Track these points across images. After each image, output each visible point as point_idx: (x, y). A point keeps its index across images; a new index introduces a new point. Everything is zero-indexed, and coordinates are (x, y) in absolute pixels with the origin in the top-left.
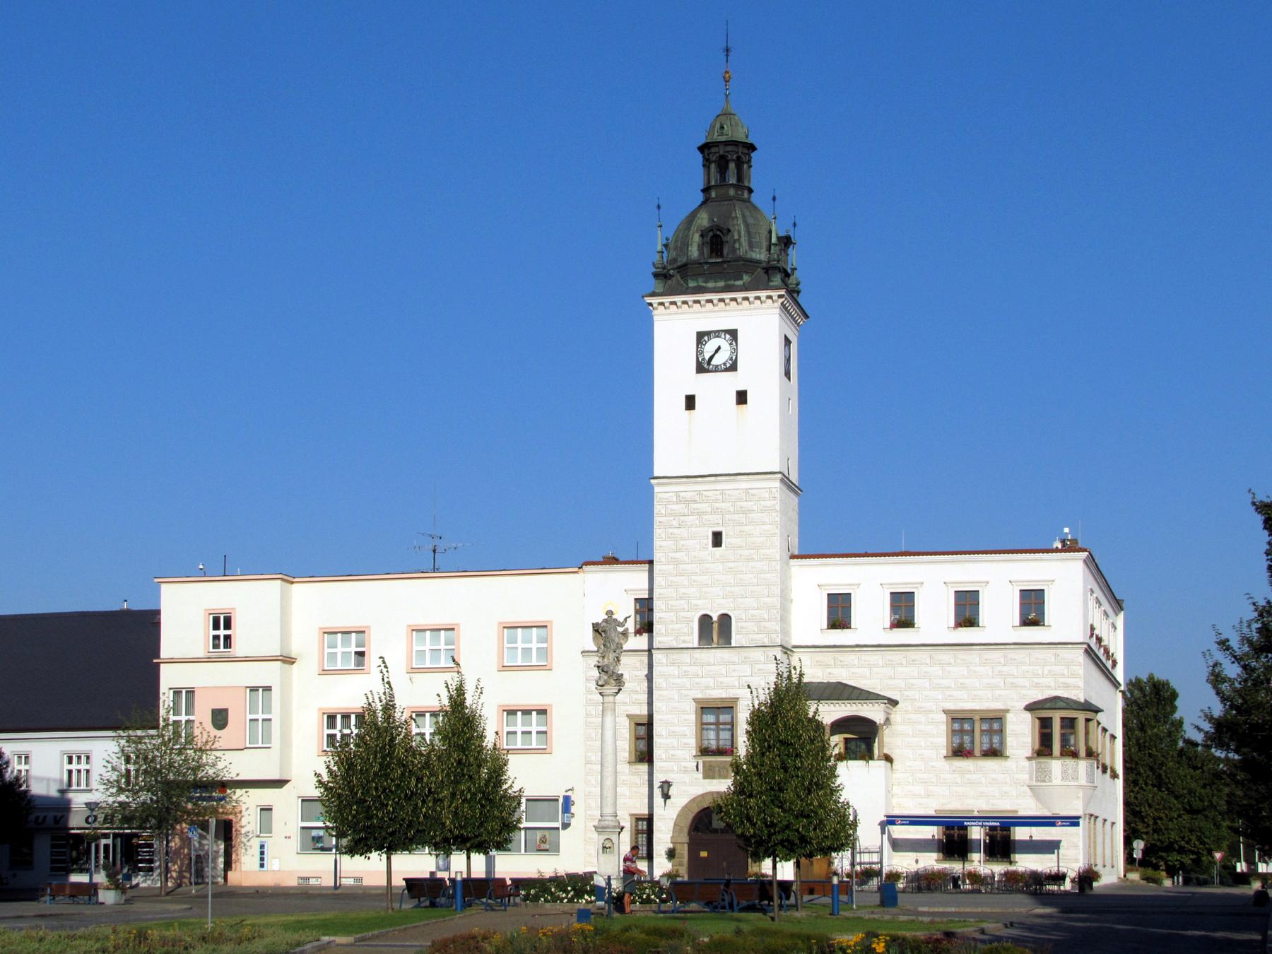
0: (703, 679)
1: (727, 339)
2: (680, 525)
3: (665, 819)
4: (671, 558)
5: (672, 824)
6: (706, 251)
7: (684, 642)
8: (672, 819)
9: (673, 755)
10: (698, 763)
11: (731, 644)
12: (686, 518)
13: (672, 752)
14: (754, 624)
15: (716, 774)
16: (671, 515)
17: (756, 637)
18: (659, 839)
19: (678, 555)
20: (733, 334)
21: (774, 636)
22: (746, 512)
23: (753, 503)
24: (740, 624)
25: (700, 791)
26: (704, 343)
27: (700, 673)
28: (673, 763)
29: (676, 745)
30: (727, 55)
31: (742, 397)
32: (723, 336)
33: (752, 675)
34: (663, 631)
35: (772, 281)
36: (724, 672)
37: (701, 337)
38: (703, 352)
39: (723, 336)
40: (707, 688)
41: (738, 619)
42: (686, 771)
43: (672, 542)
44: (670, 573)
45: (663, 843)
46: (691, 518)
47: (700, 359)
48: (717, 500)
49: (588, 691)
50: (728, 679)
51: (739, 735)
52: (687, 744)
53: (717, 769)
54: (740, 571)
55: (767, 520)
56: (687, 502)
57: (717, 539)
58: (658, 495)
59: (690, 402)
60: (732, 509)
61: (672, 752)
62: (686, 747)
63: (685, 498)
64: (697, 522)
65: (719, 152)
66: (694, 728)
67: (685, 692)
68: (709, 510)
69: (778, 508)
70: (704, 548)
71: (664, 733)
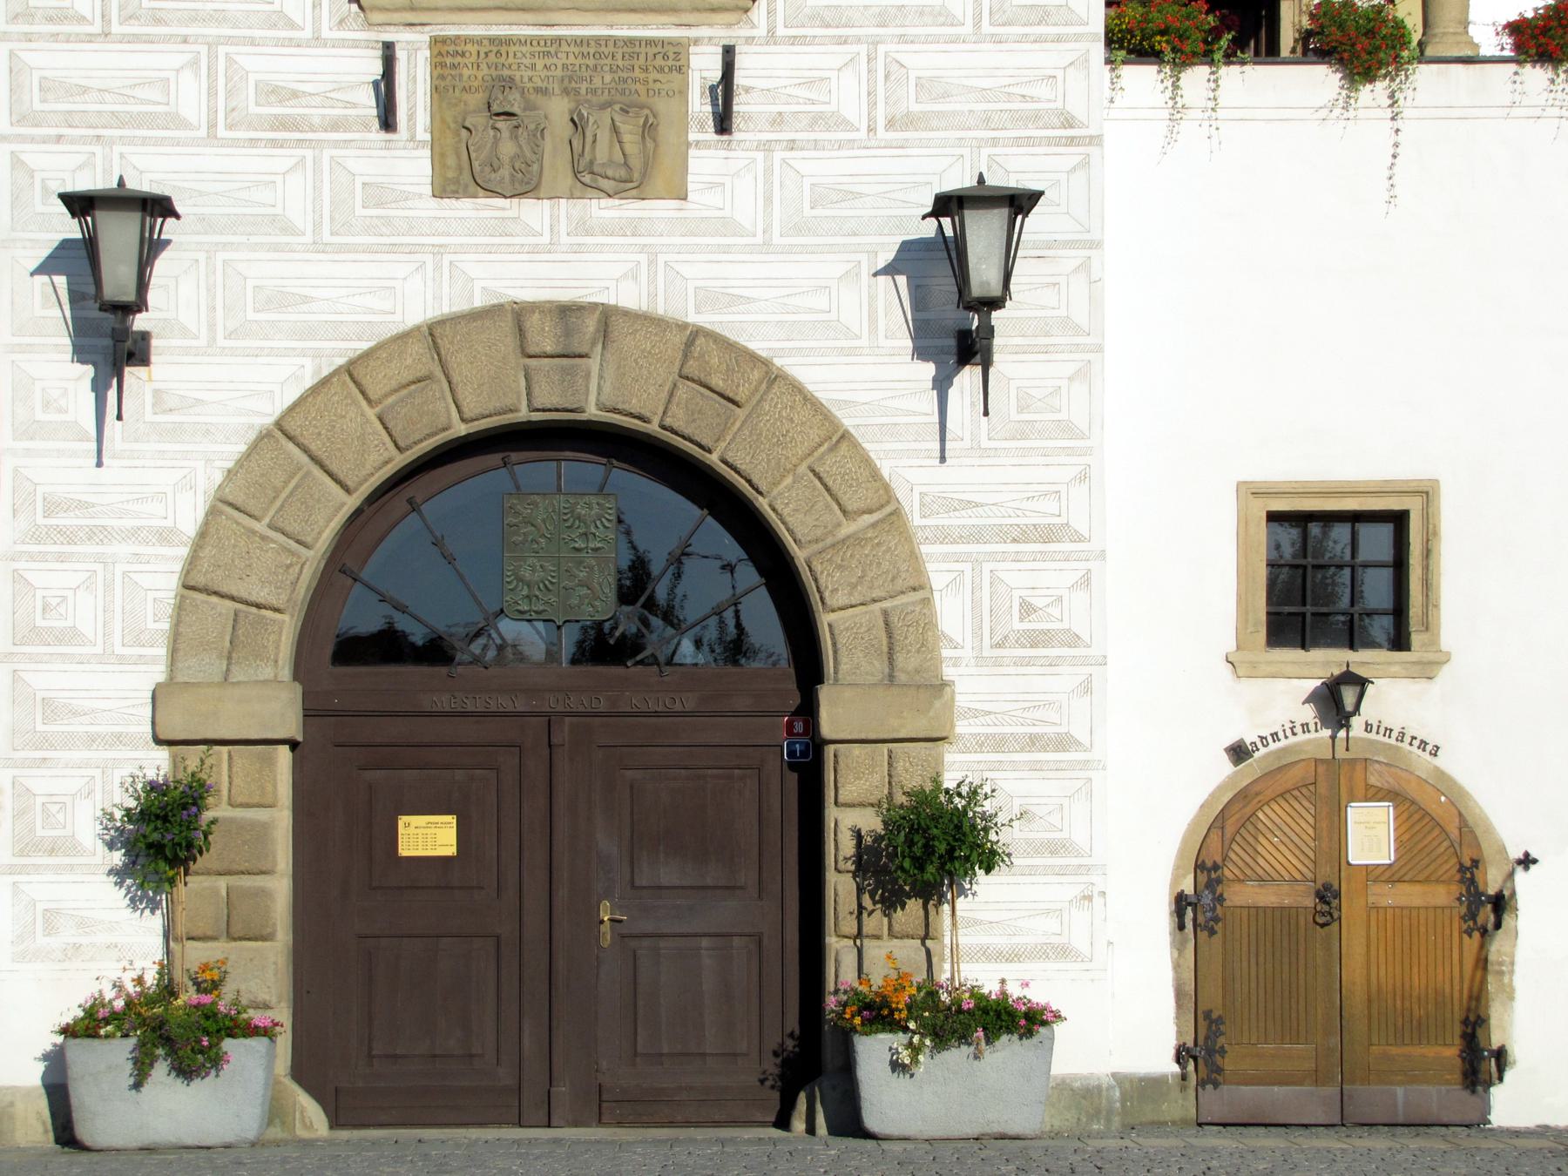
3: (99, 534)
5: (163, 581)
8: (165, 536)
10: (389, 54)
28: (168, 59)
45: (92, 740)
53: (558, 109)
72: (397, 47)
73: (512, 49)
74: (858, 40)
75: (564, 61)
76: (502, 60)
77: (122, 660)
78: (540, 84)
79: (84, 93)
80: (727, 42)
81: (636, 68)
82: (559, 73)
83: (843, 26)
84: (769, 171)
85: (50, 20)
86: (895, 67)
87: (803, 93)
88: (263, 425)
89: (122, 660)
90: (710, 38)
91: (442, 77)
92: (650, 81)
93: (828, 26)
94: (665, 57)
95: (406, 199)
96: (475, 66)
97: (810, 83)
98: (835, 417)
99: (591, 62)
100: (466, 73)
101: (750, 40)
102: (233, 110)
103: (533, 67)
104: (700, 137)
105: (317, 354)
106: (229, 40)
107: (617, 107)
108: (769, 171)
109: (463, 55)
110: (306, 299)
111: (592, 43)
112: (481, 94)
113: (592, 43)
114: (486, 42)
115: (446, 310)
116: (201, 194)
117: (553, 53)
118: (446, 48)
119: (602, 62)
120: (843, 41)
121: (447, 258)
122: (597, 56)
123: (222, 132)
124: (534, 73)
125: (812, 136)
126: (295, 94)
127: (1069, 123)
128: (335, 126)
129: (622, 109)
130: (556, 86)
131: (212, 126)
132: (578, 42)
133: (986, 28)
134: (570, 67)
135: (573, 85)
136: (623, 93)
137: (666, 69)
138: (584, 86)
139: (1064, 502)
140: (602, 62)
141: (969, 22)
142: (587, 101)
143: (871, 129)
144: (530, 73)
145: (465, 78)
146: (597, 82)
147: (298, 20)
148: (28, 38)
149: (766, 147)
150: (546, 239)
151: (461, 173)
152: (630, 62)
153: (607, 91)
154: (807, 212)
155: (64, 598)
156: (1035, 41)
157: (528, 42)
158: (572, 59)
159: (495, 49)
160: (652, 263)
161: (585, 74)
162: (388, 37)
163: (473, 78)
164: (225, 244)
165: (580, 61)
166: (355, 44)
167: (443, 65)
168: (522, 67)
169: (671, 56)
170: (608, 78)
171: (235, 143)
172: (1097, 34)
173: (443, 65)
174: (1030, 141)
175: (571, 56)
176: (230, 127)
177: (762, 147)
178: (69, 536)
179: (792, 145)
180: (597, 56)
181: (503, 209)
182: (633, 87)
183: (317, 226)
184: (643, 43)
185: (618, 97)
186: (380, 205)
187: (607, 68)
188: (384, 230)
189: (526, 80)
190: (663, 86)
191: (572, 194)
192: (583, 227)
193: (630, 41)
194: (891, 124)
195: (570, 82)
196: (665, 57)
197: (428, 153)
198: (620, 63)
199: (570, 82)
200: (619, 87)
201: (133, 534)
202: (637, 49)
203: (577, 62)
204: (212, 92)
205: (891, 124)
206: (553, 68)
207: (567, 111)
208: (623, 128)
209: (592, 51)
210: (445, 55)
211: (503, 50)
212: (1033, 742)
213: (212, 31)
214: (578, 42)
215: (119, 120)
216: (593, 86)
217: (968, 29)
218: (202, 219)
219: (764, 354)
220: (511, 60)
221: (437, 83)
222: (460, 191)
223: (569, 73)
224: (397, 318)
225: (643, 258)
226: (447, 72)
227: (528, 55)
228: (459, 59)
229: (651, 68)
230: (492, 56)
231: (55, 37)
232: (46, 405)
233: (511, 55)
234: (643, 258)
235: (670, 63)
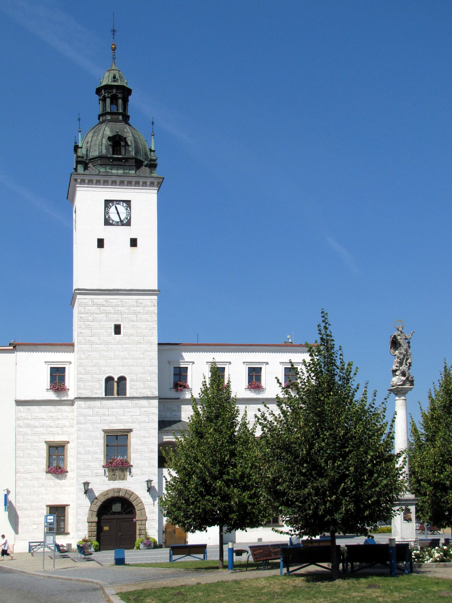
0: (108, 417)
1: (124, 206)
2: (93, 320)
3: (83, 506)
4: (88, 340)
6: (111, 150)
7: (96, 393)
8: (88, 506)
9: (89, 466)
10: (105, 470)
11: (125, 394)
12: (98, 315)
13: (88, 464)
14: (141, 383)
15: (118, 478)
16: (87, 313)
17: (142, 391)
19: (93, 339)
20: (128, 203)
21: (154, 390)
22: (136, 313)
23: (141, 308)
24: (132, 383)
25: (106, 488)
26: (109, 207)
27: (107, 413)
28: (89, 471)
29: (90, 459)
30: (114, 34)
31: (134, 243)
32: (122, 204)
33: (140, 415)
34: (83, 387)
35: (153, 173)
36: (122, 413)
37: (108, 203)
38: (108, 213)
39: (122, 204)
40: (111, 422)
41: (131, 380)
42: (97, 475)
43: (89, 330)
44: (87, 350)
45: (82, 522)
46: (101, 316)
47: (107, 217)
48: (118, 305)
49: (19, 426)
50: (124, 417)
52: (98, 458)
54: (132, 350)
55: (150, 319)
56: (99, 305)
57: (117, 330)
58: (80, 300)
59: (101, 243)
60: (127, 311)
61: (88, 464)
62: (97, 460)
63: (97, 303)
64: (105, 319)
65: (113, 92)
68: (113, 311)
69: (156, 311)
70: (109, 335)
128: (101, 475)
201: (85, 506)
215: (84, 476)
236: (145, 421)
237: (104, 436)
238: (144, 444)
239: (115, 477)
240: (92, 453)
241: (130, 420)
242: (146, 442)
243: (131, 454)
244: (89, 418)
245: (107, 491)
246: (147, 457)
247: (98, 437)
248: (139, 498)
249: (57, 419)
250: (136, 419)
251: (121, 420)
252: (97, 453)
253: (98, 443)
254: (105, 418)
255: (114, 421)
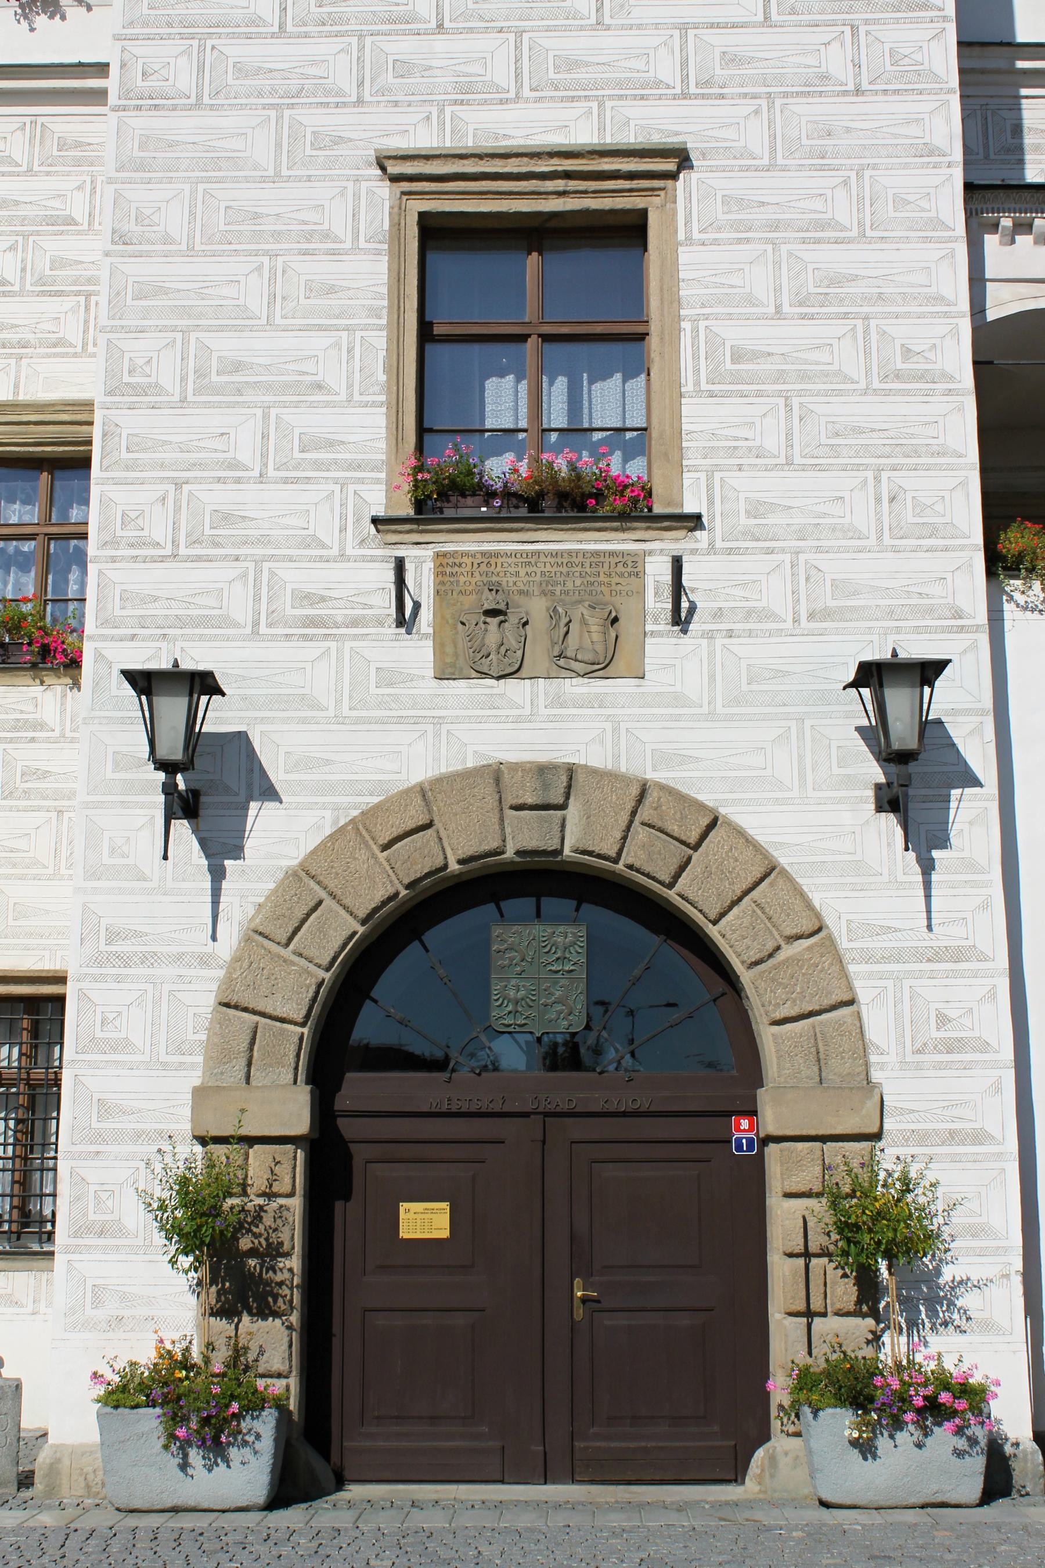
0: (440, 44)
9: (225, 518)
10: (400, 566)
15: (538, 654)
18: (105, 1109)
29: (246, 453)
51: (688, 387)
52: (331, 444)
62: (317, 465)
66: (380, 341)
67: (314, 119)
71: (167, 374)
72: (407, 561)
73: (500, 560)
74: (783, 550)
75: (543, 569)
76: (492, 569)
77: (165, 1066)
78: (522, 587)
79: (154, 601)
80: (675, 554)
81: (601, 574)
82: (538, 578)
83: (770, 540)
84: (711, 654)
85: (132, 546)
86: (813, 572)
87: (739, 592)
88: (289, 867)
89: (165, 1066)
90: (662, 550)
91: (443, 583)
92: (613, 584)
93: (758, 540)
94: (625, 564)
95: (412, 680)
96: (470, 574)
97: (744, 585)
98: (772, 856)
99: (564, 570)
100: (462, 579)
101: (694, 552)
102: (273, 612)
103: (517, 574)
104: (655, 628)
105: (336, 808)
106: (272, 558)
107: (586, 604)
108: (711, 654)
109: (460, 565)
110: (328, 762)
111: (566, 555)
112: (474, 596)
113: (566, 555)
114: (479, 556)
115: (443, 770)
116: (244, 678)
117: (533, 563)
118: (446, 560)
119: (573, 570)
120: (771, 551)
121: (445, 728)
122: (569, 565)
123: (263, 629)
124: (518, 579)
125: (748, 626)
126: (323, 599)
127: (958, 615)
128: (355, 623)
129: (590, 606)
130: (535, 588)
131: (256, 624)
132: (554, 554)
133: (887, 540)
134: (547, 574)
135: (550, 587)
136: (591, 593)
137: (626, 575)
138: (558, 589)
139: (970, 926)
140: (573, 570)
141: (873, 537)
142: (561, 600)
143: (796, 620)
144: (514, 579)
145: (461, 584)
146: (569, 585)
147: (327, 541)
148: (113, 559)
149: (709, 635)
150: (527, 711)
151: (457, 659)
152: (596, 570)
153: (577, 592)
154: (745, 687)
155: (120, 1013)
156: (928, 551)
157: (513, 555)
158: (548, 568)
159: (486, 561)
160: (616, 730)
161: (559, 579)
162: (400, 553)
163: (468, 583)
164: (263, 718)
165: (555, 569)
166: (373, 559)
167: (444, 574)
168: (508, 574)
169: (630, 564)
170: (578, 582)
171: (274, 638)
172: (977, 545)
173: (444, 574)
174: (927, 629)
175: (548, 565)
176: (270, 625)
177: (706, 636)
178: (125, 961)
179: (730, 634)
180: (569, 565)
181: (492, 687)
182: (599, 589)
183: (338, 702)
184: (607, 555)
185: (587, 597)
186: (390, 685)
187: (577, 574)
188: (393, 705)
189: (511, 584)
190: (623, 588)
191: (549, 674)
192: (559, 701)
193: (596, 553)
194: (811, 616)
195: (547, 585)
196: (625, 564)
197: (431, 643)
198: (588, 570)
199: (547, 585)
200: (588, 589)
202: (602, 559)
203: (553, 570)
204: (257, 598)
205: (811, 616)
206: (533, 574)
207: (544, 608)
208: (591, 621)
209: (565, 561)
210: (445, 565)
211: (493, 561)
212: (953, 1137)
213: (259, 551)
214: (554, 554)
215: (181, 622)
216: (566, 589)
217: (872, 541)
218: (244, 698)
219: (711, 804)
220: (499, 569)
221: (438, 588)
222: (457, 673)
223: (546, 578)
224: (403, 776)
225: (608, 726)
226: (447, 579)
227: (513, 565)
228: (456, 569)
229: (613, 574)
230: (483, 567)
231: (135, 558)
232: (112, 851)
233: (499, 565)
234: (608, 726)
235: (629, 569)
236: (825, 77)
237: (397, 226)
238: (825, 299)
239: (512, 641)
240: (269, 388)
241: (666, 70)
242: (836, 281)
243: (688, 408)
244: (235, 50)
245: (424, 792)
246: (858, 431)
247: (326, 236)
248: (784, 873)
249: (52, 221)
250: (730, 59)
251: (573, 65)
252: (319, 387)
253: (331, 290)
254: (401, 47)
255: (502, 74)
